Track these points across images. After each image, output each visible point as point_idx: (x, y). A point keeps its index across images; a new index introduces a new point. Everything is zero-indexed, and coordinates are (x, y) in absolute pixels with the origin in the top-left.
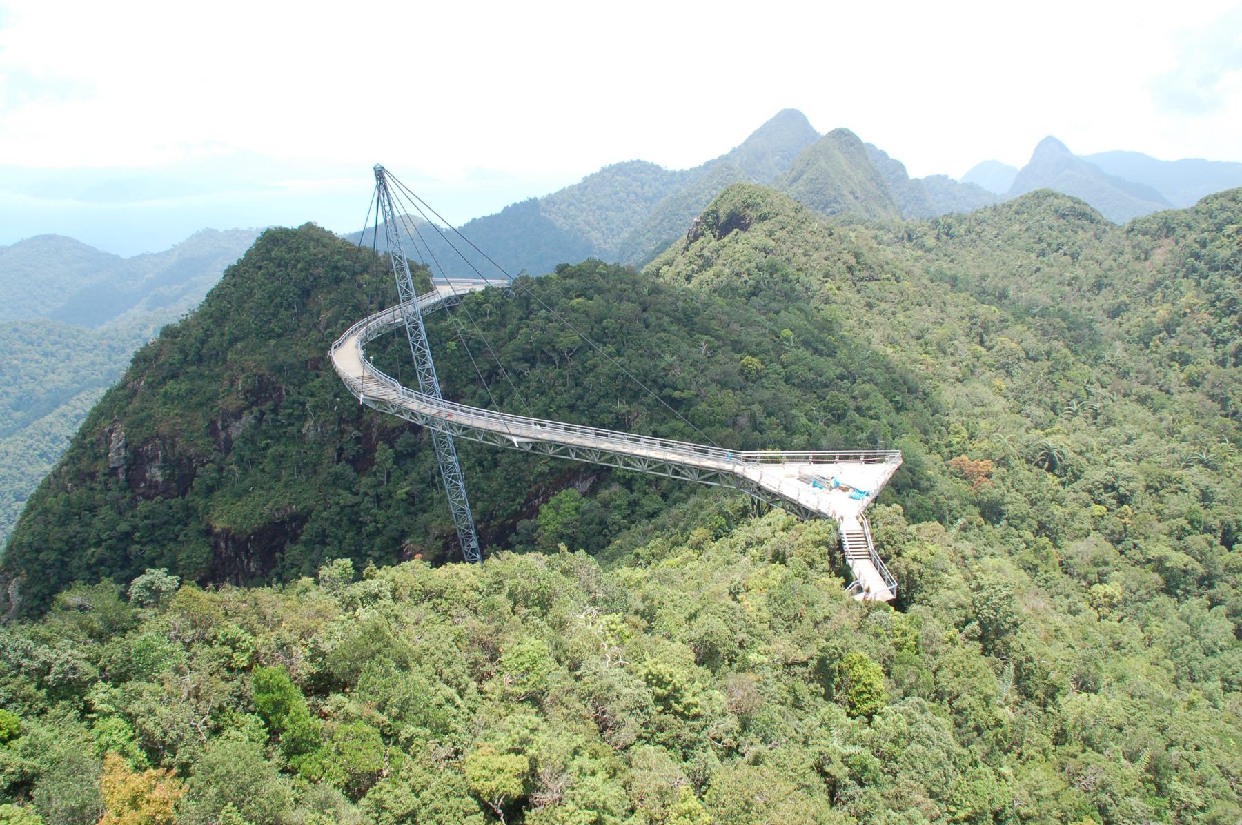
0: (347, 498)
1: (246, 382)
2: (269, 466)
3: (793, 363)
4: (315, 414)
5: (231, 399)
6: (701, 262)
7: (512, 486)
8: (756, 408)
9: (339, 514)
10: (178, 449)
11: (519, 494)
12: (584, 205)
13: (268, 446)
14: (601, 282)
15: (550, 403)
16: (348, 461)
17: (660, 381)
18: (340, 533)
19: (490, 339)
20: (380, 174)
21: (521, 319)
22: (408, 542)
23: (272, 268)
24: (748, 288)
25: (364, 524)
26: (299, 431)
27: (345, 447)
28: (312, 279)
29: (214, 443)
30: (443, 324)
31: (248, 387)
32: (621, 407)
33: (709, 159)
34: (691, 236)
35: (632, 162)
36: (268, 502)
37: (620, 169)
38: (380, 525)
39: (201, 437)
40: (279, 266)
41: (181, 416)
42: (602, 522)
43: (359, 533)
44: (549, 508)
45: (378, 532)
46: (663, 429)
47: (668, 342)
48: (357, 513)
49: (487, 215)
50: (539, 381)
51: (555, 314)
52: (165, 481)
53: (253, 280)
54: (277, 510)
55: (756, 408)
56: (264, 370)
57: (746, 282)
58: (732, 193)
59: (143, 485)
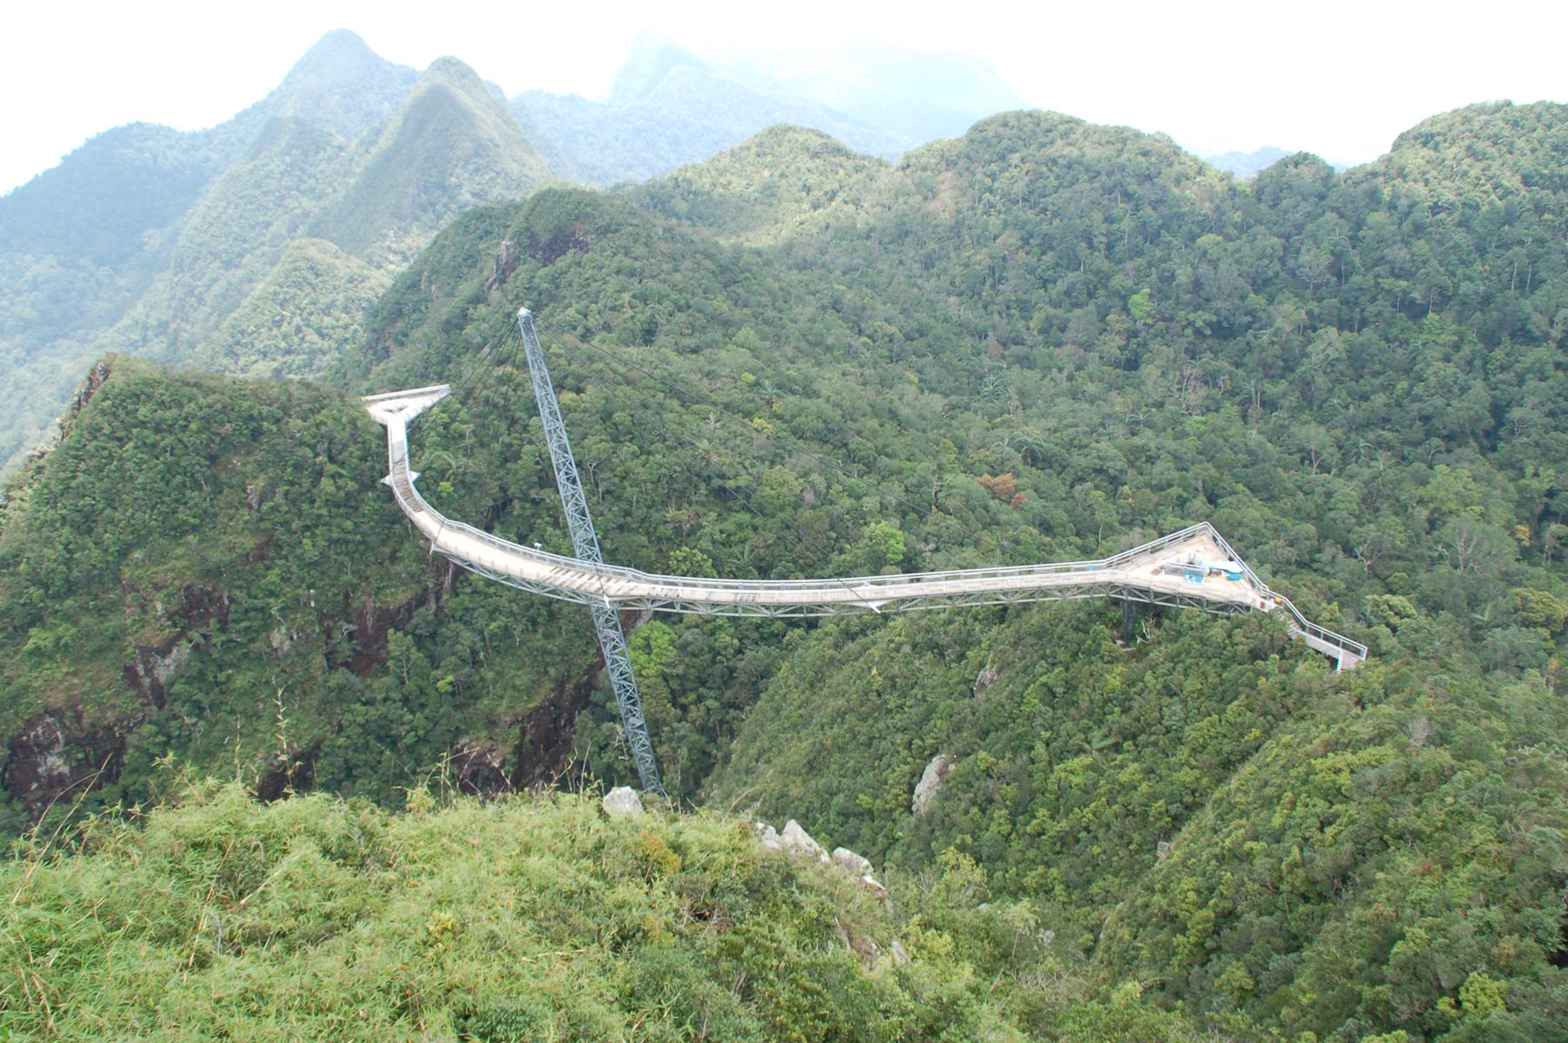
4: (285, 617)
5: (148, 632)
10: (86, 721)
16: (346, 664)
17: (705, 474)
28: (218, 440)
29: (138, 696)
33: (239, 110)
37: (116, 137)
38: (421, 733)
39: (117, 694)
41: (75, 674)
42: (712, 649)
52: (72, 770)
56: (190, 578)
59: (35, 786)
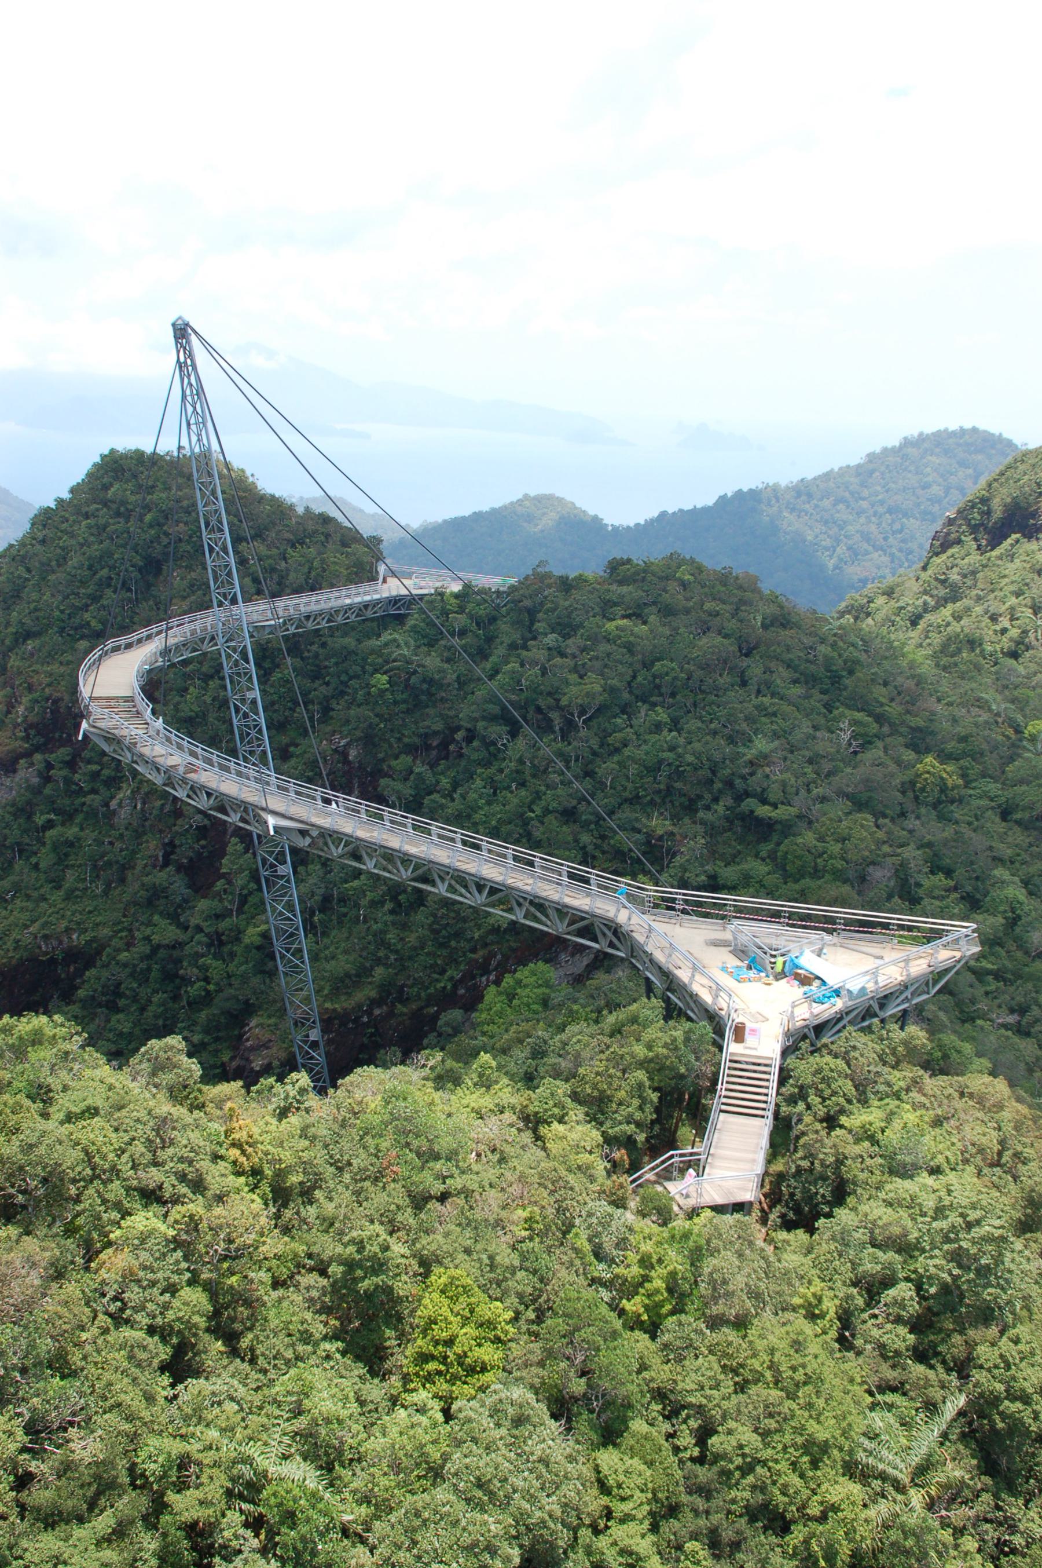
0: (166, 932)
1: (28, 709)
2: (45, 858)
3: (1022, 782)
6: (942, 592)
7: (442, 945)
8: (911, 853)
9: (148, 957)
11: (452, 960)
12: (864, 504)
13: (50, 825)
14: (674, 595)
15: (533, 802)
16: (180, 868)
18: (144, 992)
19: (451, 677)
20: (182, 332)
21: (513, 646)
22: (253, 1023)
23: (104, 515)
24: (1006, 643)
25: (186, 981)
26: (107, 805)
27: (177, 842)
30: (374, 643)
31: (32, 718)
32: (658, 824)
34: (937, 543)
35: (963, 431)
36: (33, 921)
38: (211, 987)
40: (118, 514)
43: (176, 998)
44: (500, 994)
45: (207, 999)
46: (729, 873)
47: (774, 714)
48: (178, 961)
49: (688, 507)
50: (521, 761)
51: (572, 645)
53: (72, 535)
54: (46, 937)
55: (911, 853)
57: (1004, 631)
58: (1022, 467)
